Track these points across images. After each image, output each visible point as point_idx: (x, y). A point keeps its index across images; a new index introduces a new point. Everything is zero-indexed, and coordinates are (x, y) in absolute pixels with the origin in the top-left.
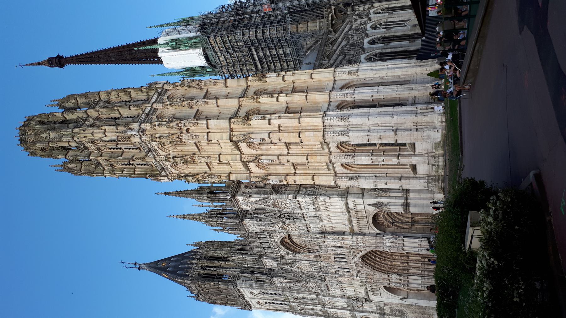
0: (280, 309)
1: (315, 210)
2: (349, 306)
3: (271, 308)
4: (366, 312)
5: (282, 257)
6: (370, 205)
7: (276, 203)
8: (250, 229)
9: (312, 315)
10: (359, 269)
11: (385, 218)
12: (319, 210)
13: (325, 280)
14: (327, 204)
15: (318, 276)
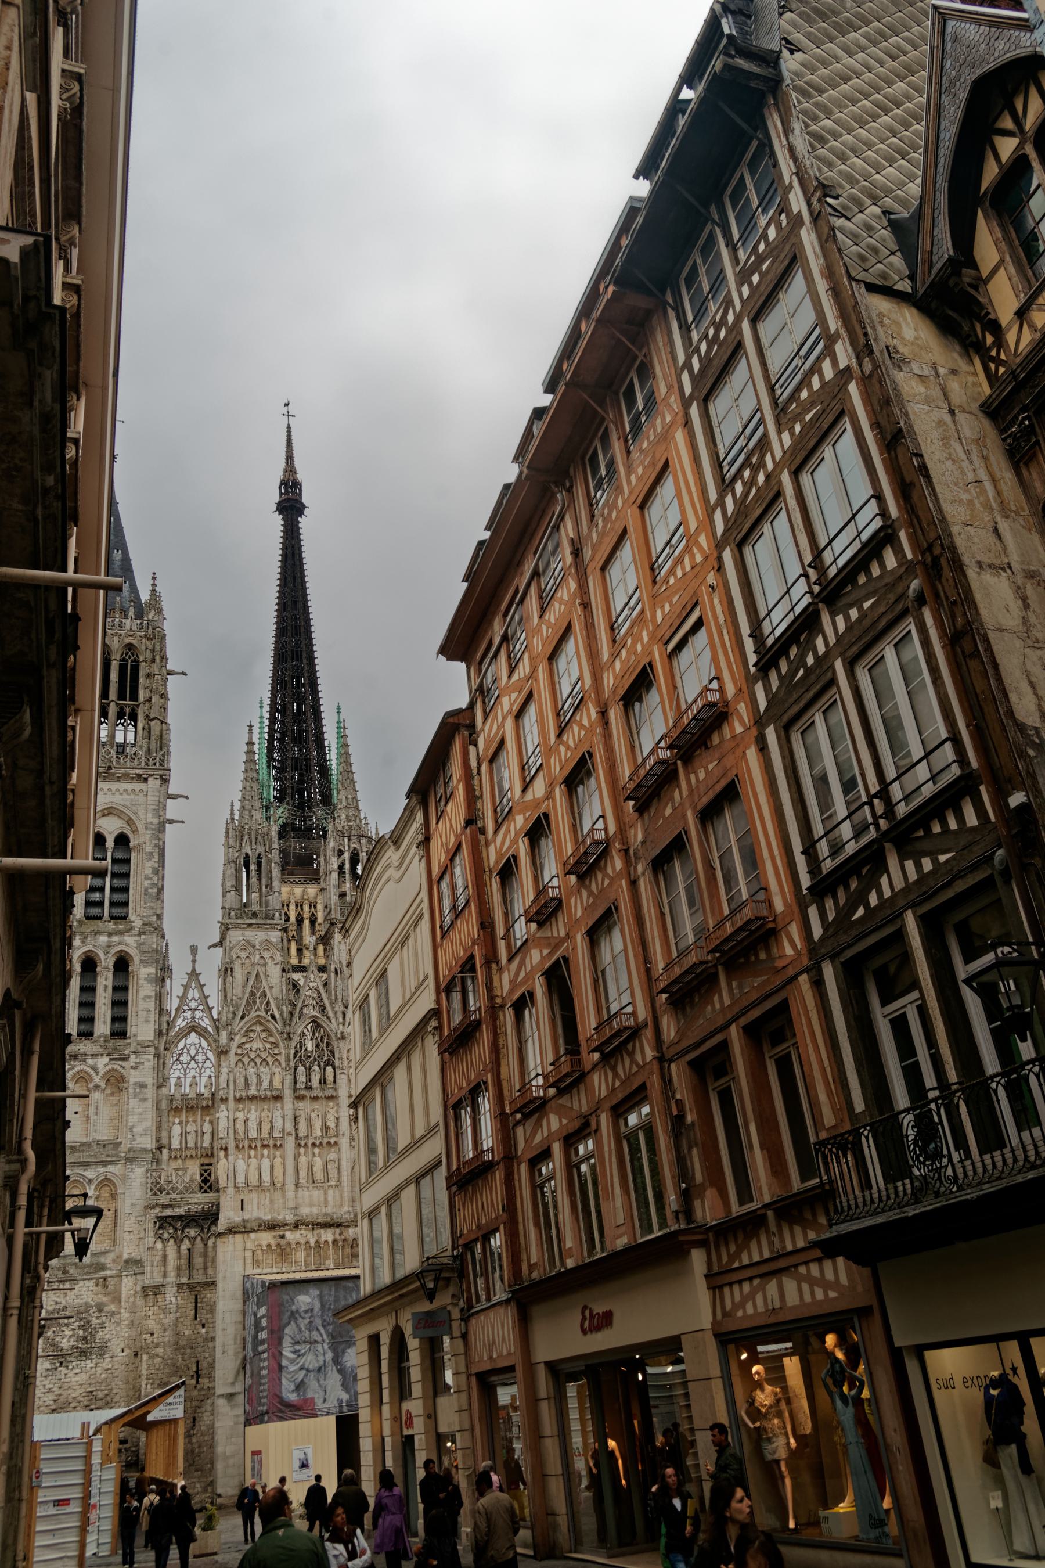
13: (300, 1098)
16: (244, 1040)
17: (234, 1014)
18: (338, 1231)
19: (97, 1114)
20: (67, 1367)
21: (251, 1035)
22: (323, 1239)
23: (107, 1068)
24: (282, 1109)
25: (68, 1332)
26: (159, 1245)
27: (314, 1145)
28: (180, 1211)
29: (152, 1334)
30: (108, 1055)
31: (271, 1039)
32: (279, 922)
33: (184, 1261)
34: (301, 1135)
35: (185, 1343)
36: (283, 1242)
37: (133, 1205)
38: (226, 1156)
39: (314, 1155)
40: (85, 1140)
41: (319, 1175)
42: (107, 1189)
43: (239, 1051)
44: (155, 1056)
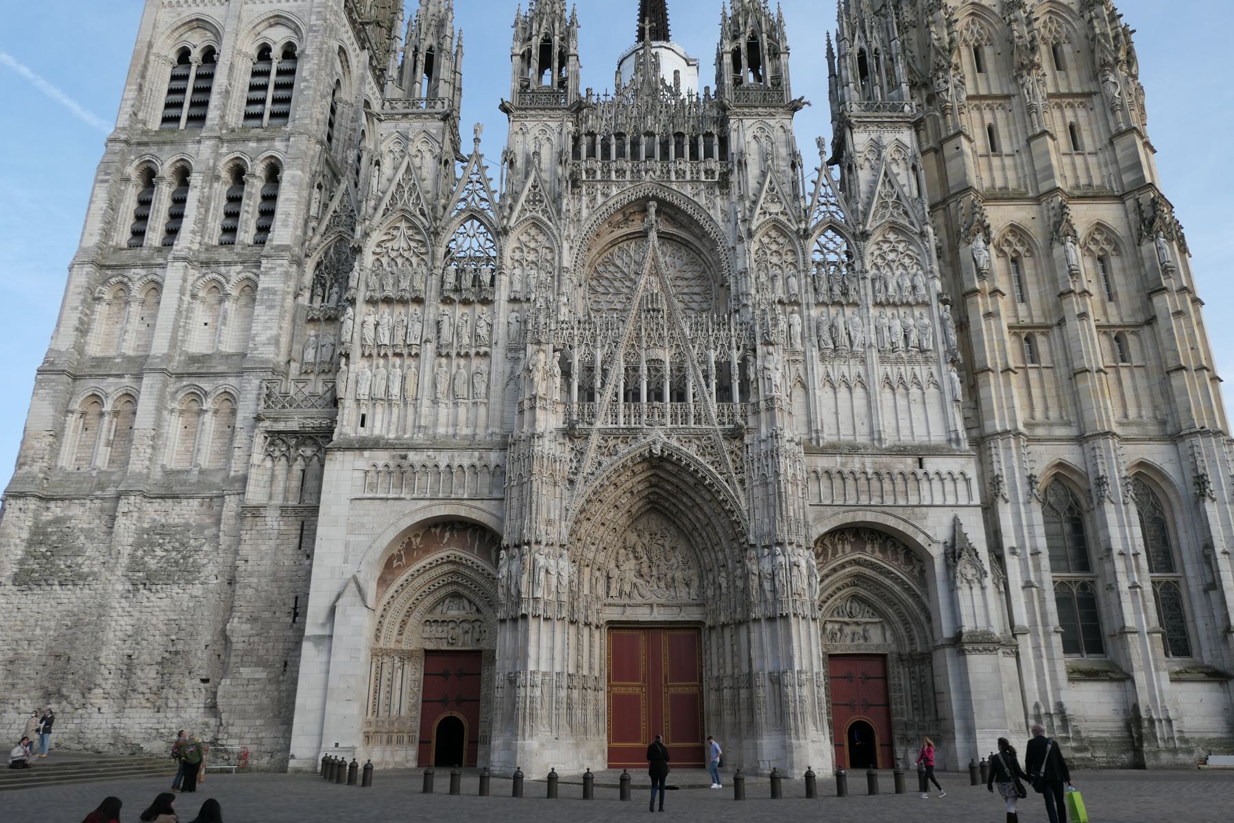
0: (145, 90)
1: (888, 346)
2: (194, 359)
3: (152, 58)
4: (158, 425)
5: (575, 183)
6: (956, 524)
7: (892, 237)
8: (747, 122)
9: (111, 201)
10: (595, 439)
11: (843, 566)
12: (883, 361)
13: (447, 301)
14: (914, 390)
15: (486, 278)
16: (385, 238)
17: (375, 209)
18: (476, 454)
19: (224, 324)
20: (150, 590)
21: (395, 233)
22: (455, 464)
23: (240, 276)
24: (423, 314)
25: (159, 552)
26: (269, 464)
27: (458, 355)
28: (294, 425)
29: (247, 561)
30: (242, 263)
31: (418, 237)
32: (441, 110)
33: (295, 484)
34: (442, 342)
35: (283, 574)
36: (405, 463)
37: (245, 418)
38: (347, 365)
39: (458, 366)
40: (210, 352)
41: (462, 389)
42: (228, 404)
43: (378, 250)
44: (292, 262)
